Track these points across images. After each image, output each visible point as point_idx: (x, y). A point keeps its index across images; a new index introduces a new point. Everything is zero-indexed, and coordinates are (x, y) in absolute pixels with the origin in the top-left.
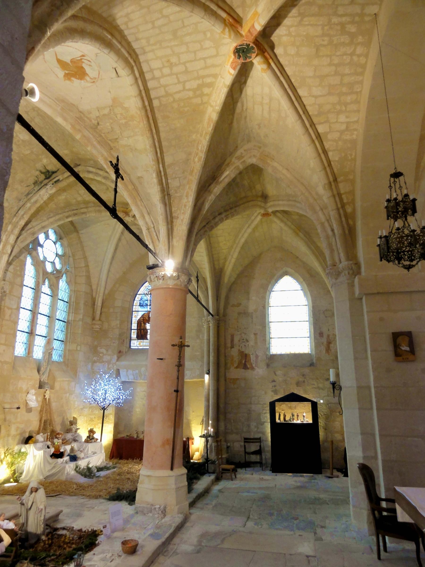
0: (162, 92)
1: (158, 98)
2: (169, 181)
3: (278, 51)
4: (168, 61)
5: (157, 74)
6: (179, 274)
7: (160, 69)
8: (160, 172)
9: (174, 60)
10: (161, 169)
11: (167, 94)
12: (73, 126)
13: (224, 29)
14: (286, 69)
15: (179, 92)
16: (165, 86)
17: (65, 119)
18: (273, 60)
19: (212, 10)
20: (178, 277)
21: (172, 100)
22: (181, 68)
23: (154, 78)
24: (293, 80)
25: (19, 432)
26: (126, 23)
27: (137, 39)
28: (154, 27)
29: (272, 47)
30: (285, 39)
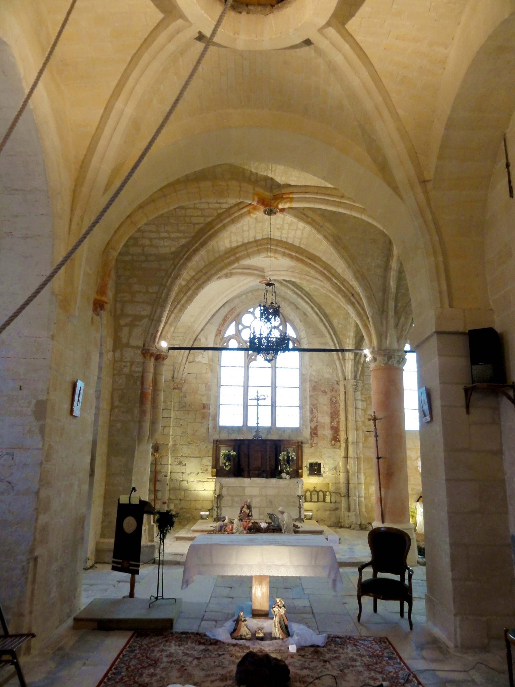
0: (298, 241)
1: (300, 243)
2: (351, 283)
3: (292, 183)
4: (278, 229)
5: (284, 235)
6: (375, 356)
7: (282, 233)
8: (336, 283)
9: (279, 226)
10: (336, 281)
11: (301, 239)
12: (300, 279)
13: (250, 216)
14: (308, 185)
15: (302, 233)
16: (294, 237)
17: (295, 277)
18: (292, 193)
19: (239, 216)
20: (375, 359)
21: (306, 239)
22: (286, 226)
23: (287, 238)
24: (319, 185)
25: (415, 492)
26: (238, 242)
27: (255, 237)
28: (249, 231)
29: (289, 186)
30: (283, 179)
